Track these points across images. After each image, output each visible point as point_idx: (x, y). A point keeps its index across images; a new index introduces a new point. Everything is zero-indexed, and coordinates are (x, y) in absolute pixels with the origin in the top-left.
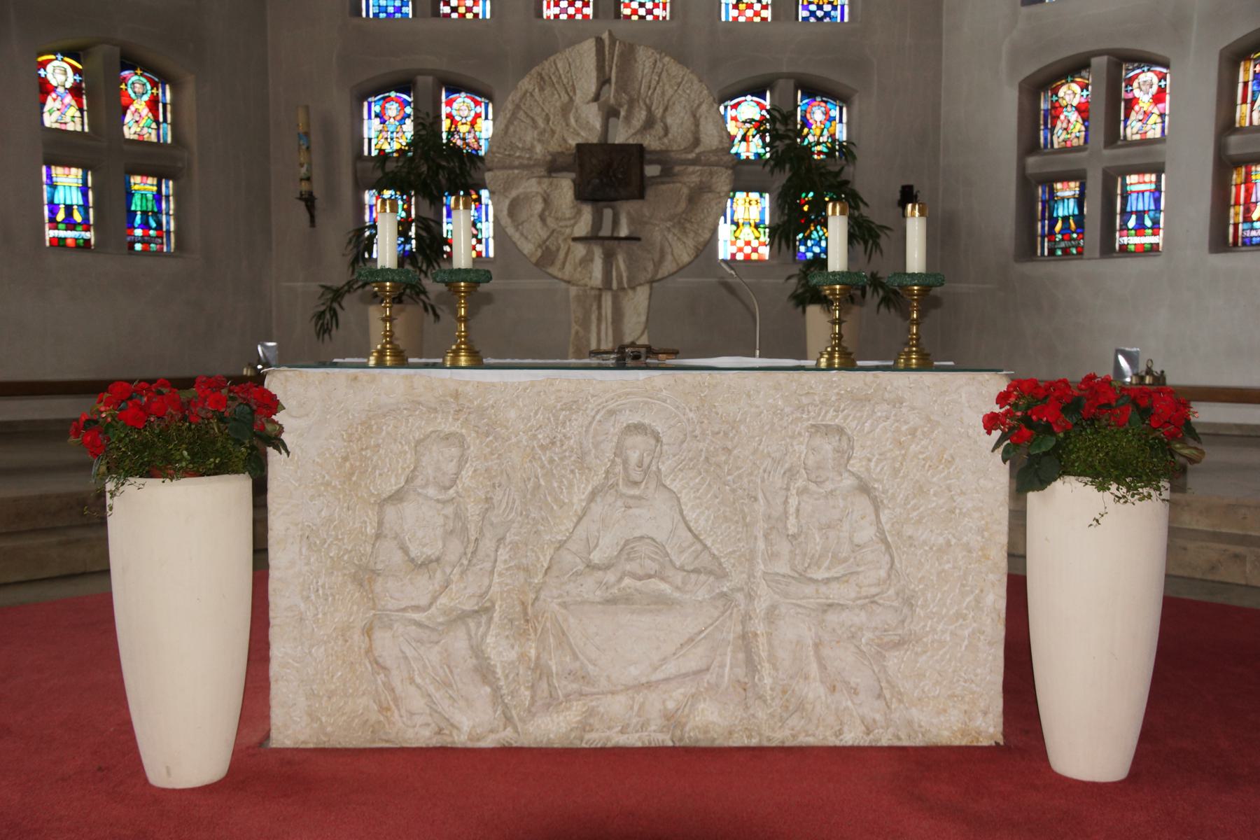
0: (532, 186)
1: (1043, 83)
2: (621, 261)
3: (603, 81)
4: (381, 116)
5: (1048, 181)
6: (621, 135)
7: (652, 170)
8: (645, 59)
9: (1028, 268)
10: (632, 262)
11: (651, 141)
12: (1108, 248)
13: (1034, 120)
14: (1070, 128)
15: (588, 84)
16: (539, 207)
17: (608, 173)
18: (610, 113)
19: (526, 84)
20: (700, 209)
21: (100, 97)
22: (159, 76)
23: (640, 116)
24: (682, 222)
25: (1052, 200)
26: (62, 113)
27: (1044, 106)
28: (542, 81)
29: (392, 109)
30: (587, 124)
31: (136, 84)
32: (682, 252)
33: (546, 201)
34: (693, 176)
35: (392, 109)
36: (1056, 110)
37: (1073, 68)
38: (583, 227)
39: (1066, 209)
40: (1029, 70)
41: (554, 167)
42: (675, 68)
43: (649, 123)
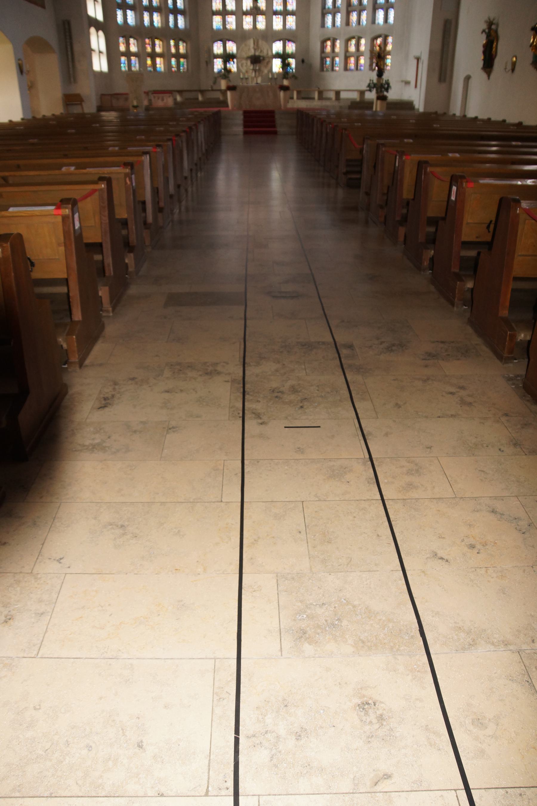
0: (244, 61)
1: (324, 42)
2: (257, 73)
3: (254, 43)
4: (217, 46)
5: (325, 58)
6: (257, 54)
7: (261, 58)
8: (260, 42)
9: (322, 73)
10: (259, 74)
11: (261, 55)
12: (333, 70)
13: (323, 47)
14: (328, 49)
15: (252, 45)
16: (245, 64)
17: (256, 60)
18: (255, 50)
19: (243, 45)
20: (270, 63)
21: (177, 47)
22: (184, 41)
23: (259, 51)
24: (266, 67)
25: (326, 61)
26: (173, 50)
27: (325, 45)
28: (246, 45)
29: (219, 45)
30: (252, 52)
31: (181, 43)
32: (266, 71)
33: (247, 63)
34: (267, 60)
35: (219, 45)
36: (326, 46)
37: (329, 39)
38: (252, 67)
39: (328, 63)
40: (322, 39)
41: (248, 58)
42: (264, 43)
43: (261, 51)
